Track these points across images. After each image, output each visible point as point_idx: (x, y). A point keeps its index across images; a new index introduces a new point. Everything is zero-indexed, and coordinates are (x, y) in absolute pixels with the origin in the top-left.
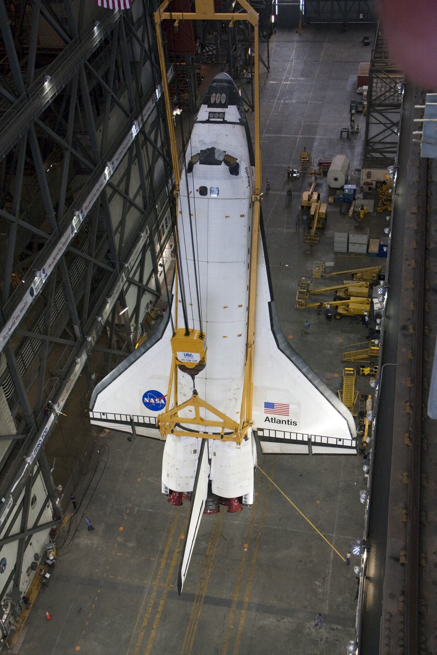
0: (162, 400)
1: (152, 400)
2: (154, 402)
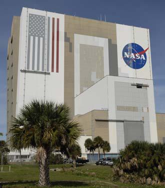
0: (143, 55)
2: (134, 57)
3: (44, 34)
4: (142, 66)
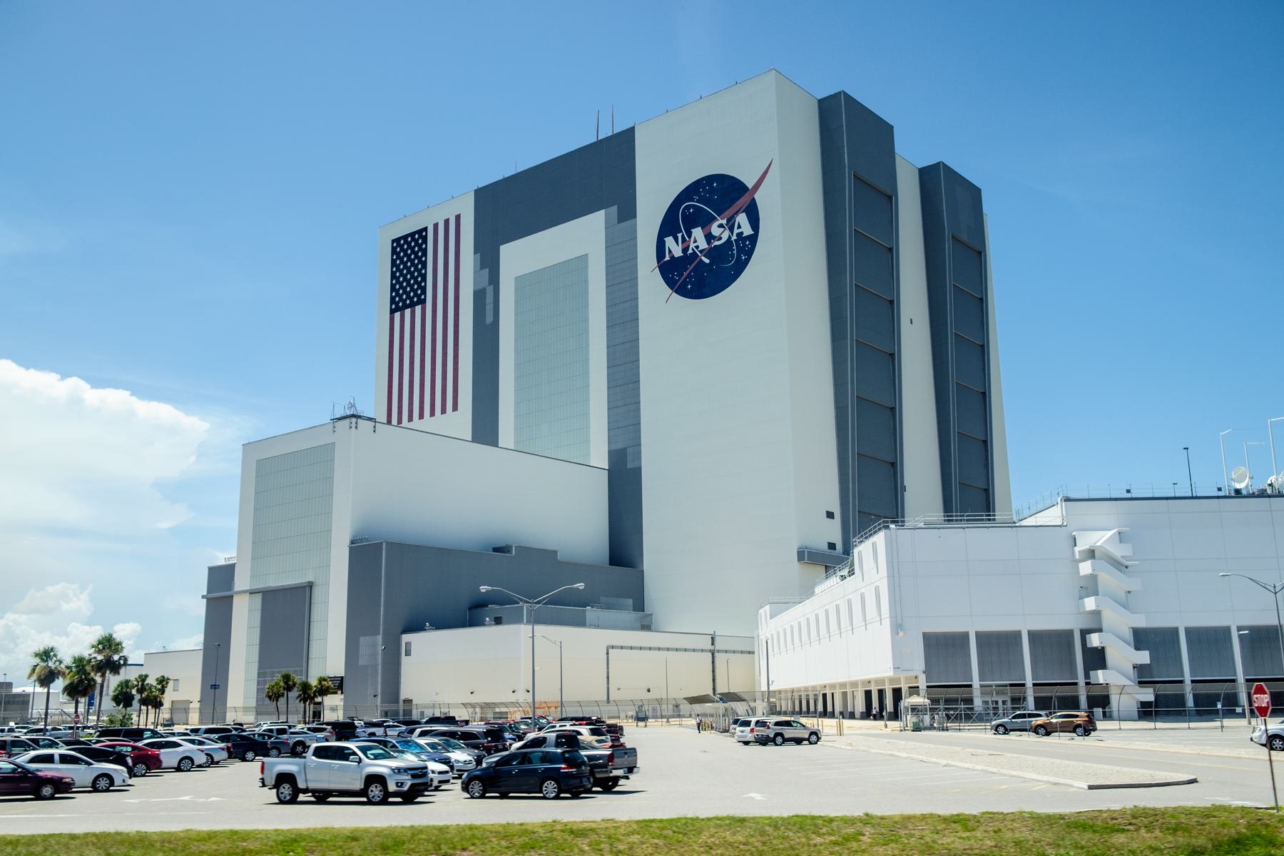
0: (742, 219)
2: (703, 244)
3: (424, 292)
4: (740, 267)
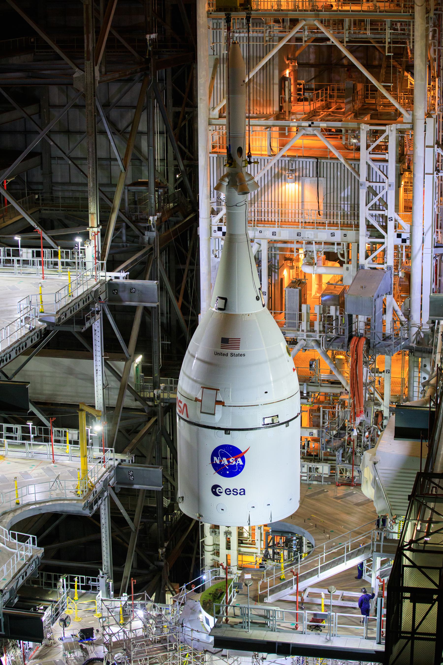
0: (239, 460)
1: (225, 461)
2: (227, 463)
4: (238, 473)
